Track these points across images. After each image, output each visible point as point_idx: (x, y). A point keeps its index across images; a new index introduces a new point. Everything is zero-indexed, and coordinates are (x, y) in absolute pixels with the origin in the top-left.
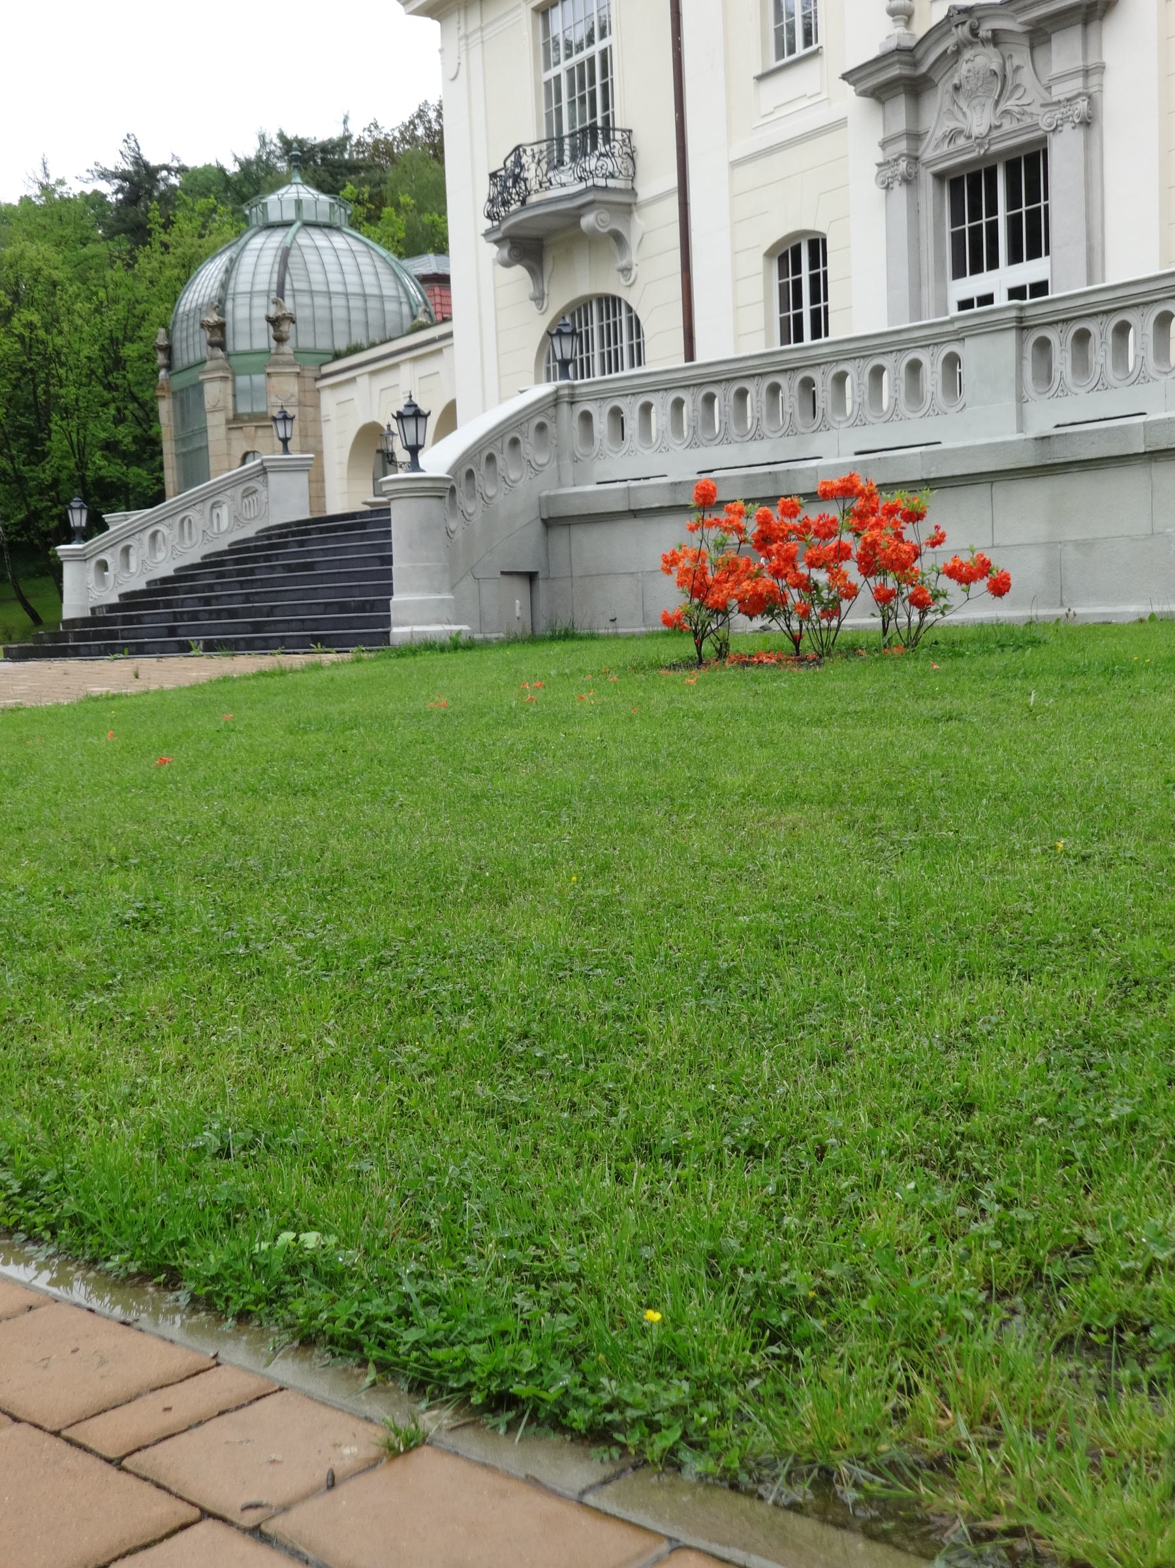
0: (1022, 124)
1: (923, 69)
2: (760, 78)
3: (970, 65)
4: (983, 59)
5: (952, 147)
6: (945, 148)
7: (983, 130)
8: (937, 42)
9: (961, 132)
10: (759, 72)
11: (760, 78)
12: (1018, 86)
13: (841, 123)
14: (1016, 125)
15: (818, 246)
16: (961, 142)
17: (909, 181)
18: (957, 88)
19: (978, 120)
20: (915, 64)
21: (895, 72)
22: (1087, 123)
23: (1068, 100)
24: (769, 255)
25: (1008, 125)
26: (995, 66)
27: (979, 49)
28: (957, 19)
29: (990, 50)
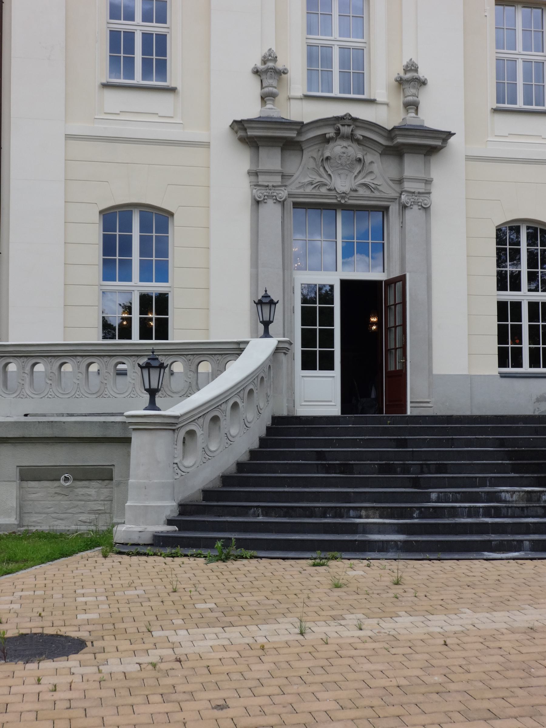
0: (372, 195)
1: (303, 138)
2: (106, 86)
3: (344, 150)
4: (354, 151)
5: (315, 192)
6: (309, 190)
7: (346, 189)
8: (318, 127)
9: (325, 185)
10: (104, 81)
11: (106, 86)
12: (371, 172)
13: (207, 145)
14: (368, 193)
15: (158, 220)
16: (323, 190)
17: (283, 203)
18: (328, 158)
19: (342, 183)
20: (299, 133)
21: (292, 134)
22: (426, 209)
23: (419, 193)
24: (101, 212)
25: (362, 192)
26: (360, 156)
27: (350, 143)
28: (347, 122)
29: (355, 145)
